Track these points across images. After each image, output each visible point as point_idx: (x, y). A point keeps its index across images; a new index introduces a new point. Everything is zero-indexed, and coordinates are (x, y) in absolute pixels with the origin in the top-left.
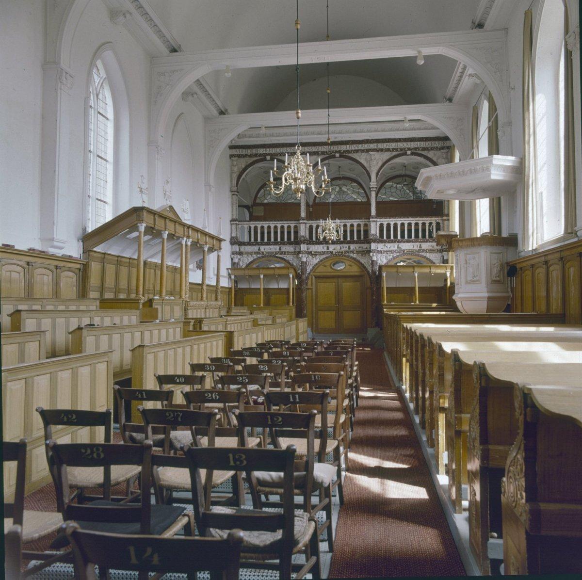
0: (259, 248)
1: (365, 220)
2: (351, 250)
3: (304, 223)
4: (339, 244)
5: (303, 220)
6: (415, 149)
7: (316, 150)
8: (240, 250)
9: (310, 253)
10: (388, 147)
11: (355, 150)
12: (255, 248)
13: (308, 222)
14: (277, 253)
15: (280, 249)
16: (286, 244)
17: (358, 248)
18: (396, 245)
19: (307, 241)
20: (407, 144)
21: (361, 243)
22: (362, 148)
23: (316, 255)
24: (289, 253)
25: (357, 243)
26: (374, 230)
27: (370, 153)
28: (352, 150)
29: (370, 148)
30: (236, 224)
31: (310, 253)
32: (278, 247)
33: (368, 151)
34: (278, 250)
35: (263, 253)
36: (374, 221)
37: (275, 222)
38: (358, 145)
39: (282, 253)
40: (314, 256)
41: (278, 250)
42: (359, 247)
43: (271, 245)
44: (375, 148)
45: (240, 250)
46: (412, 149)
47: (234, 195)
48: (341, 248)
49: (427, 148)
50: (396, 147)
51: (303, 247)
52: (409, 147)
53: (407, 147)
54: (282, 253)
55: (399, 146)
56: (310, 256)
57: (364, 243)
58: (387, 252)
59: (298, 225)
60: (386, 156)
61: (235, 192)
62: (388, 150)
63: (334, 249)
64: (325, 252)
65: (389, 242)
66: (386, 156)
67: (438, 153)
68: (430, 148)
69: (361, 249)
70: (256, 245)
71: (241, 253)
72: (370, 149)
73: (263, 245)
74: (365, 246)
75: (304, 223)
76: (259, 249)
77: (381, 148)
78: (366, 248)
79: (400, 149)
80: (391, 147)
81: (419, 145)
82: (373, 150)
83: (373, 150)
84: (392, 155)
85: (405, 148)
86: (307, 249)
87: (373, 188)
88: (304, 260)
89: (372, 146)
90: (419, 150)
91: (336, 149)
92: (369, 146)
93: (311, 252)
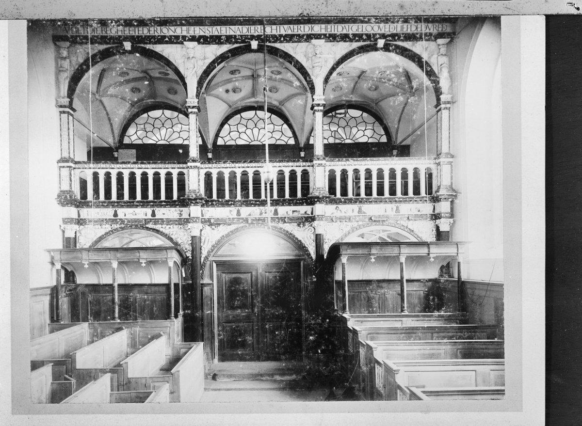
0: (116, 211)
1: (304, 163)
2: (279, 216)
3: (196, 167)
4: (259, 205)
5: (194, 161)
6: (394, 36)
7: (216, 34)
8: (79, 216)
9: (208, 222)
10: (345, 32)
11: (286, 36)
12: (108, 213)
13: (202, 166)
14: (147, 221)
15: (153, 214)
16: (165, 206)
17: (290, 213)
18: (355, 207)
19: (201, 199)
20: (379, 27)
21: (296, 204)
22: (300, 32)
23: (219, 224)
24: (169, 222)
25: (289, 205)
26: (319, 182)
27: (314, 41)
28: (281, 36)
29: (313, 32)
30: (70, 167)
31: (208, 222)
32: (149, 211)
33: (309, 37)
34: (149, 216)
35: (122, 221)
36: (320, 165)
37: (143, 166)
38: (292, 26)
39: (156, 222)
40: (213, 227)
41: (149, 216)
42: (293, 211)
43: (137, 206)
44: (323, 32)
45: (79, 216)
46: (389, 36)
47: (64, 112)
48: (261, 214)
49: (413, 34)
50: (360, 32)
51: (195, 210)
52: (383, 32)
53: (379, 32)
54: (156, 222)
55: (364, 30)
56: (208, 228)
57: (302, 204)
58: (341, 219)
59: (185, 171)
60: (344, 48)
61: (65, 107)
62: (345, 38)
63: (250, 215)
64: (233, 219)
65: (345, 202)
66: (344, 48)
67: (432, 45)
68: (418, 36)
69: (296, 214)
70: (107, 206)
71: (80, 222)
72: (313, 34)
73: (122, 206)
74: (304, 209)
75: (196, 167)
76: (116, 215)
77: (333, 32)
78: (306, 213)
79: (366, 35)
80: (351, 32)
81: (399, 29)
82: (318, 36)
83: (318, 36)
84: (351, 49)
85: (374, 35)
86: (203, 216)
87: (318, 105)
88: (196, 233)
89: (317, 29)
90: (399, 39)
91: (253, 31)
92: (312, 29)
93: (209, 220)
